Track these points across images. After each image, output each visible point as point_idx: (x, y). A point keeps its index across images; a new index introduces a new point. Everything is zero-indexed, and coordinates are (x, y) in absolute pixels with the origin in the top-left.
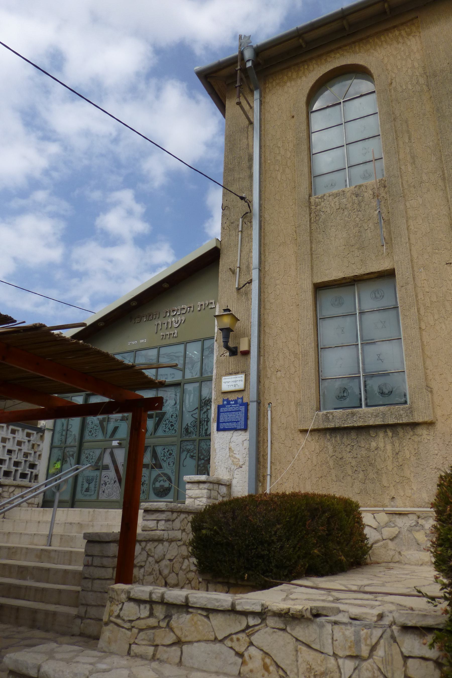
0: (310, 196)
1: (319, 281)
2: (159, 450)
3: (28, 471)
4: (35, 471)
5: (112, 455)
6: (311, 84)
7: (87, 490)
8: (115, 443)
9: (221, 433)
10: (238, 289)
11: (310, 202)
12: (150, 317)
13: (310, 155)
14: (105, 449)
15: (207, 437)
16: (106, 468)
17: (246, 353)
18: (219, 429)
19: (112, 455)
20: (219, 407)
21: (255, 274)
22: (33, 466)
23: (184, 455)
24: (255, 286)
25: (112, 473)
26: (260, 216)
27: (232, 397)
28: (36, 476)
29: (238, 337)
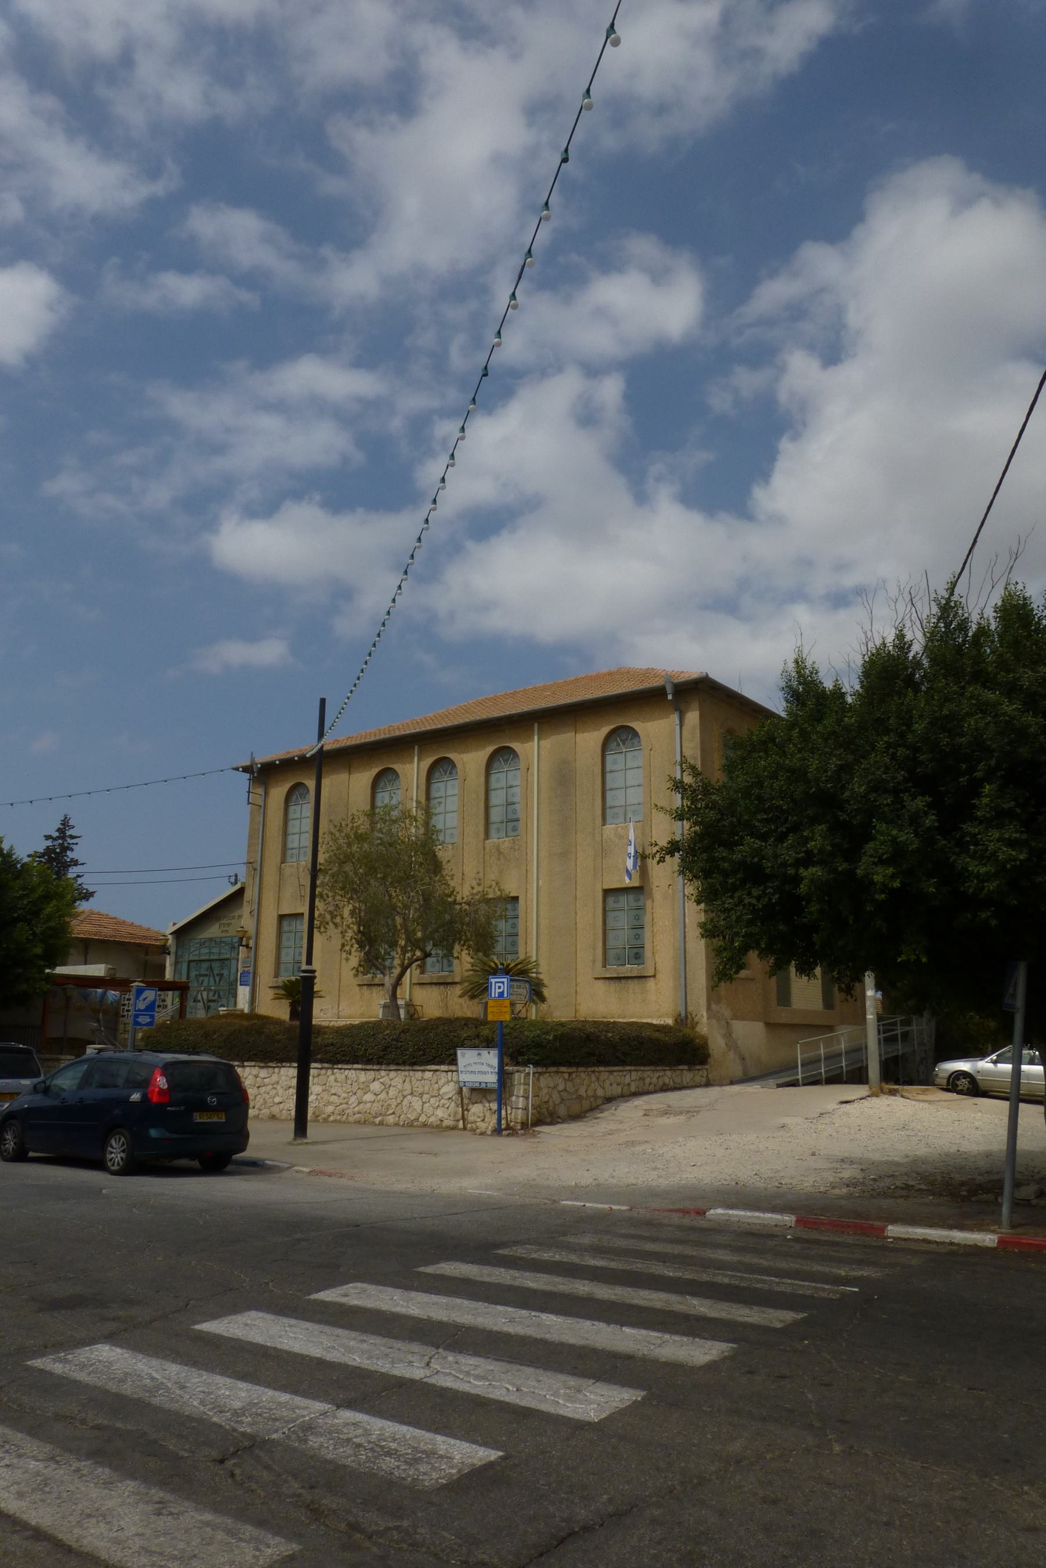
0: (282, 862)
1: (282, 913)
2: (221, 992)
3: (161, 1004)
4: (165, 1003)
5: (201, 994)
6: (287, 790)
7: (191, 1013)
8: (202, 988)
9: (242, 987)
10: (251, 912)
11: (280, 869)
12: (218, 919)
13: (285, 834)
14: (198, 992)
15: (236, 989)
16: (199, 1001)
17: (251, 948)
18: (241, 985)
19: (201, 994)
20: (241, 974)
21: (256, 905)
22: (164, 1001)
23: (230, 995)
24: (256, 911)
25: (201, 1004)
26: (261, 870)
27: (246, 969)
28: (166, 1006)
29: (249, 938)
